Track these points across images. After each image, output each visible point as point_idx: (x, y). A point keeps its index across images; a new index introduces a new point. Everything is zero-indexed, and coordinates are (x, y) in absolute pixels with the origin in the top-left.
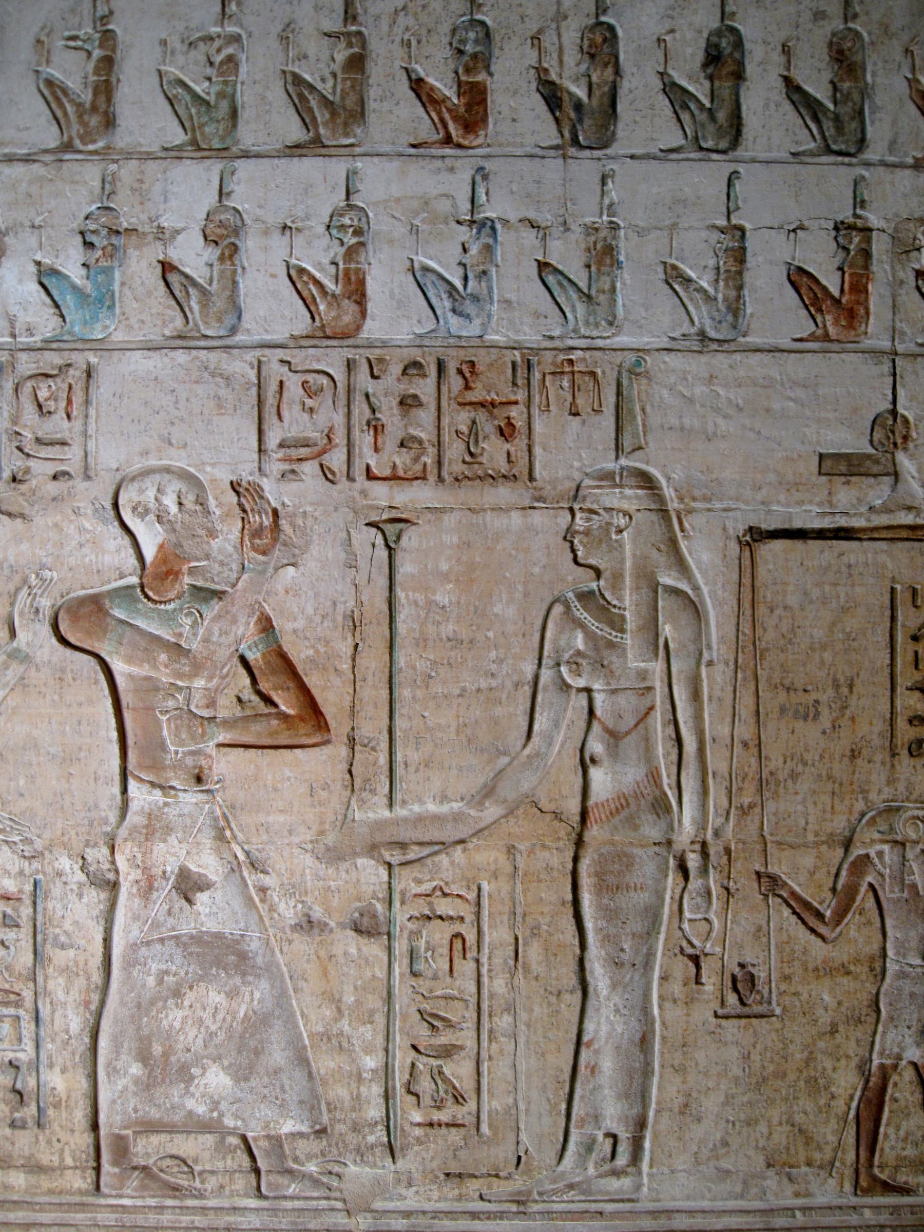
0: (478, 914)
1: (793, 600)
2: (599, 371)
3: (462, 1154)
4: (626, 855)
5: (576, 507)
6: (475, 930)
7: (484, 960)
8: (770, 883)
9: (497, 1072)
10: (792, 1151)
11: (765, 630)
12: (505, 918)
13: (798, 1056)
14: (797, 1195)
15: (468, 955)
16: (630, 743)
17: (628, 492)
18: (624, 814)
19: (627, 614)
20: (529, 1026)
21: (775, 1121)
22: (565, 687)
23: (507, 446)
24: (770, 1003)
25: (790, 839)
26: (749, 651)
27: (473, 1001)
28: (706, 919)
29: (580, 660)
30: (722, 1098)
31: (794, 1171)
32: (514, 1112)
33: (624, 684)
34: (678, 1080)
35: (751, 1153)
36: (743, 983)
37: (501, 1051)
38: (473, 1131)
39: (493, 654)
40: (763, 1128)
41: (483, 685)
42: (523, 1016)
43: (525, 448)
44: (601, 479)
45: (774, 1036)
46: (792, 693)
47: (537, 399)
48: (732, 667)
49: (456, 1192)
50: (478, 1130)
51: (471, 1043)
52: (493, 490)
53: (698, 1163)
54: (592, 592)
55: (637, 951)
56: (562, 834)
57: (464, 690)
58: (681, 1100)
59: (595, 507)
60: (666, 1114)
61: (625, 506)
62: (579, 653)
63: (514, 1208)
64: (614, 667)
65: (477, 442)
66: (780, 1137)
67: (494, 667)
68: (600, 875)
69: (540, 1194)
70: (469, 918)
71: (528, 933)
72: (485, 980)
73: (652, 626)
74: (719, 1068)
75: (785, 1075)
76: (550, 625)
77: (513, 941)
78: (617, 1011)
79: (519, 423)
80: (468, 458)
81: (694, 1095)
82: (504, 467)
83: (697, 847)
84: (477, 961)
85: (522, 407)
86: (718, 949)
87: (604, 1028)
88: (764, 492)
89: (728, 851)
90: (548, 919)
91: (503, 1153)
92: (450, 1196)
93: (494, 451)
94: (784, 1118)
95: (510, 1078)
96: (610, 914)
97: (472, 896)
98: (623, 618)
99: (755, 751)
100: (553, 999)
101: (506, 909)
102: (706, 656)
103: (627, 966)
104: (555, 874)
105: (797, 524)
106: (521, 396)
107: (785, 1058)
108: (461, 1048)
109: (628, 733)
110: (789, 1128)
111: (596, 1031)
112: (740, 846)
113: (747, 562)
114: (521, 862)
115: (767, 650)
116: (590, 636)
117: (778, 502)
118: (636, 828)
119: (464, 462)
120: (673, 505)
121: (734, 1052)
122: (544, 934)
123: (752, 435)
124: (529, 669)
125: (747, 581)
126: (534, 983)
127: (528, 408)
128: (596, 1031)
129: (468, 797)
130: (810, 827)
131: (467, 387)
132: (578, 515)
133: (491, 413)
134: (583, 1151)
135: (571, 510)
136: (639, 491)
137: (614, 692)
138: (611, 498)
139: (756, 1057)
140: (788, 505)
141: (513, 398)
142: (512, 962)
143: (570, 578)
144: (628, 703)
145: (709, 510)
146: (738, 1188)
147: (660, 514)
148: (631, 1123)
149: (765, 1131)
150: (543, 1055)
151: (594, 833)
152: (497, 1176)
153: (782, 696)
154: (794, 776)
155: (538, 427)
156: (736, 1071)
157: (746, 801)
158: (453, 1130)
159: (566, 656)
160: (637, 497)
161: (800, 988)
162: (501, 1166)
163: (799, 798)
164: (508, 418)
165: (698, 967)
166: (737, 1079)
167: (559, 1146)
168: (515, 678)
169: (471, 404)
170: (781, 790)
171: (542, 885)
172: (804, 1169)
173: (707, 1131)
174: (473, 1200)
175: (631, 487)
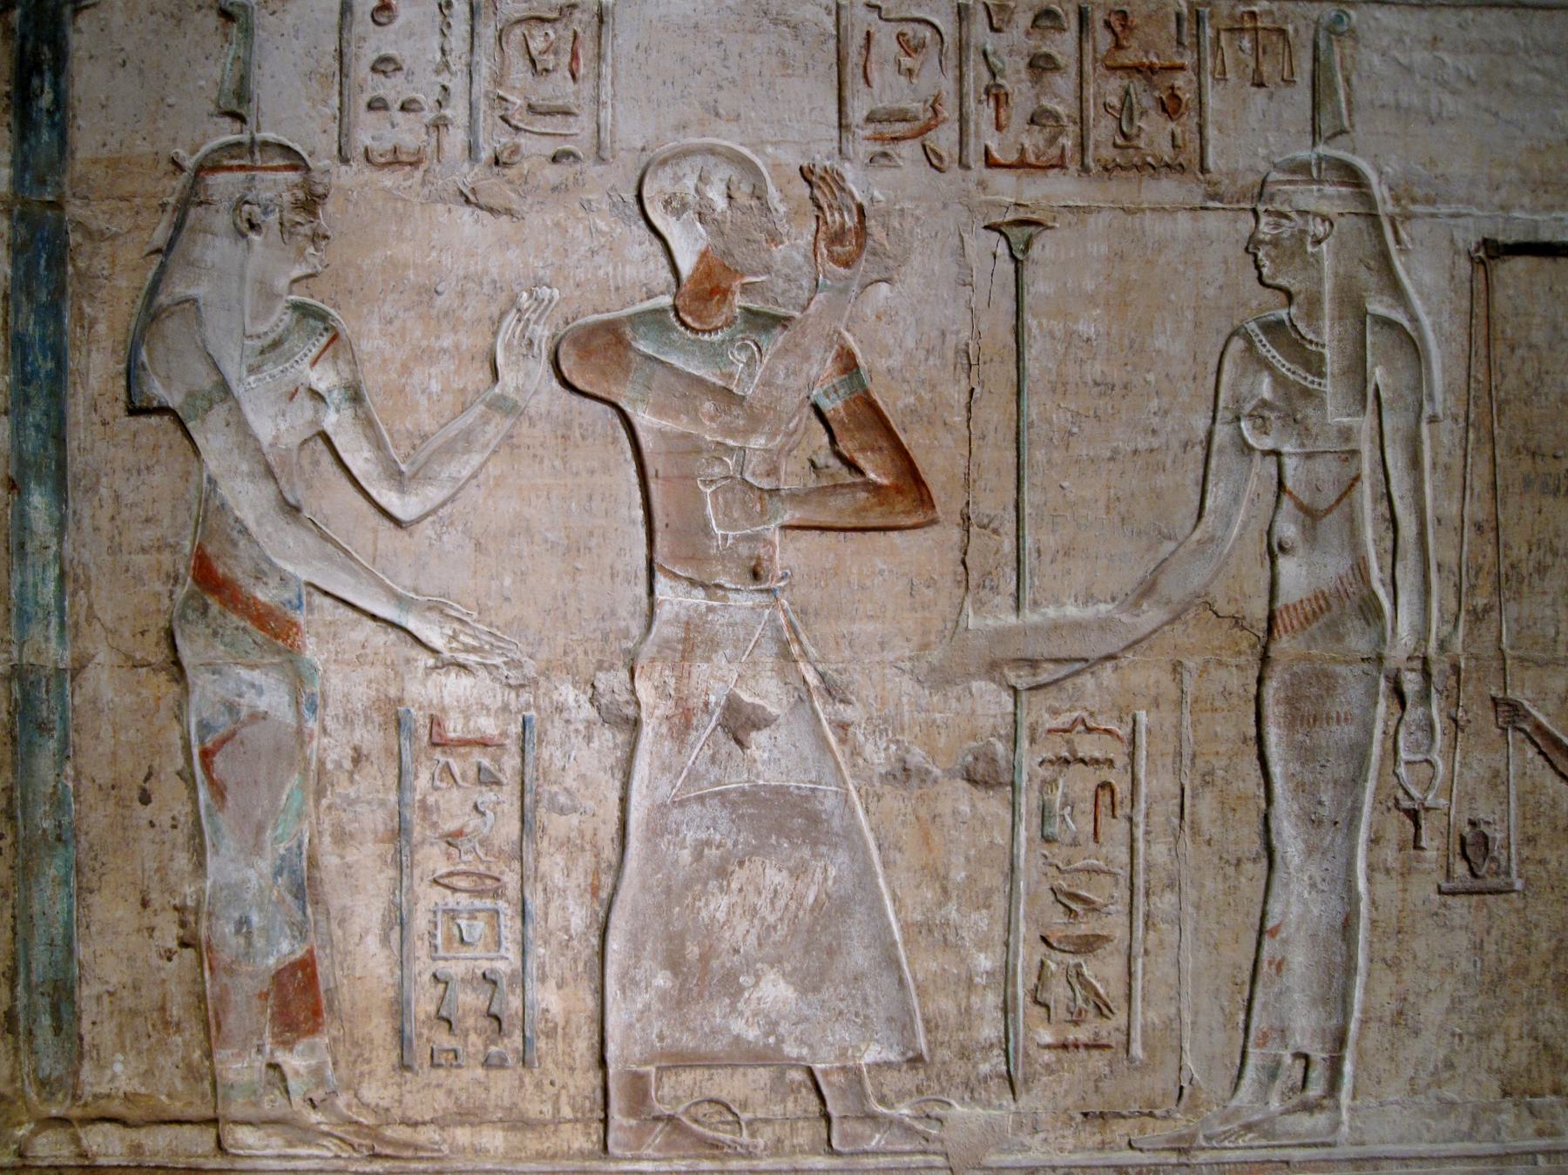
0: (1132, 756)
1: (1538, 337)
2: (1290, 28)
3: (1105, 1085)
4: (1326, 676)
5: (1261, 208)
6: (1128, 778)
7: (1140, 818)
8: (1510, 712)
9: (1153, 972)
10: (1535, 1074)
11: (1504, 376)
12: (1169, 760)
13: (1544, 945)
14: (1540, 1133)
15: (1118, 812)
16: (1331, 525)
17: (1329, 190)
18: (1323, 620)
19: (1327, 352)
20: (1198, 907)
21: (1514, 1034)
22: (1246, 449)
23: (1171, 125)
24: (1508, 874)
25: (1537, 654)
26: (1485, 404)
27: (1124, 874)
28: (1427, 761)
29: (1267, 413)
30: (1447, 1002)
31: (1537, 1100)
32: (1175, 1025)
33: (1321, 446)
34: (1391, 978)
35: (1483, 1076)
36: (1474, 847)
37: (1161, 942)
38: (1122, 1054)
39: (1154, 404)
40: (1498, 1043)
41: (1142, 445)
42: (1190, 893)
43: (1195, 129)
44: (1294, 172)
45: (1514, 918)
46: (1538, 459)
47: (1209, 63)
48: (1462, 424)
49: (1098, 1138)
50: (1128, 1052)
51: (1120, 933)
52: (1153, 183)
53: (1414, 1092)
54: (1280, 323)
55: (1340, 804)
56: (1244, 646)
57: (1115, 451)
58: (1394, 1005)
59: (1286, 208)
60: (1374, 1025)
61: (1325, 208)
62: (1264, 404)
63: (1173, 1158)
64: (1310, 422)
65: (1131, 120)
66: (1520, 1056)
67: (1155, 421)
68: (1292, 702)
69: (1208, 1138)
70: (1121, 761)
71: (1198, 781)
72: (1141, 845)
73: (1357, 369)
74: (1444, 962)
75: (1527, 970)
76: (1227, 366)
77: (1178, 791)
78: (1313, 885)
79: (1187, 96)
80: (1120, 141)
81: (1411, 999)
82: (1167, 153)
83: (1417, 664)
84: (1130, 820)
85: (1190, 74)
86: (1443, 802)
87: (1295, 909)
88: (1503, 192)
89: (1456, 669)
90: (1224, 763)
91: (1160, 1082)
92: (1090, 1144)
93: (1155, 132)
94: (1526, 1029)
95: (1173, 980)
96: (1305, 754)
97: (1124, 731)
98: (1321, 357)
99: (1491, 535)
100: (1231, 871)
101: (1170, 748)
102: (1427, 410)
103: (1327, 823)
104: (1235, 700)
105: (1545, 236)
106: (1188, 59)
107: (1528, 948)
108: (1107, 939)
109: (1329, 510)
110: (1531, 1043)
111: (1284, 914)
112: (1473, 663)
113: (1481, 286)
114: (1189, 684)
115: (1507, 402)
116: (1279, 381)
117: (1522, 207)
118: (1340, 638)
119: (1115, 145)
120: (1386, 208)
121: (1462, 940)
122: (1219, 782)
123: (1487, 117)
124: (1201, 424)
125: (1480, 310)
126: (1205, 848)
127: (1198, 75)
128: (1284, 914)
129: (1121, 597)
130: (1561, 637)
131: (1118, 46)
132: (1264, 219)
133: (1149, 80)
134: (1264, 1078)
135: (1255, 211)
136: (1344, 190)
137: (1309, 456)
138: (1307, 197)
139: (1490, 947)
140: (1534, 211)
141: (1178, 61)
142: (1176, 821)
143: (1254, 303)
144: (1327, 471)
145: (1433, 215)
146: (1465, 1126)
147: (1370, 220)
148: (1329, 1038)
149: (1501, 1046)
150: (1216, 946)
151: (1284, 645)
152: (1151, 1115)
153: (1526, 464)
154: (1541, 569)
155: (1211, 100)
156: (1465, 965)
157: (1480, 602)
158: (1095, 1053)
159: (1248, 408)
160: (1340, 196)
161: (1547, 854)
162: (1159, 1100)
163: (1548, 599)
164: (1172, 88)
165: (1417, 826)
166: (1465, 978)
167: (1235, 1072)
168: (1183, 436)
169: (1123, 68)
170: (1525, 588)
171: (1218, 716)
172: (1550, 1098)
173: (1428, 1048)
174: (1120, 1149)
175: (1333, 184)
